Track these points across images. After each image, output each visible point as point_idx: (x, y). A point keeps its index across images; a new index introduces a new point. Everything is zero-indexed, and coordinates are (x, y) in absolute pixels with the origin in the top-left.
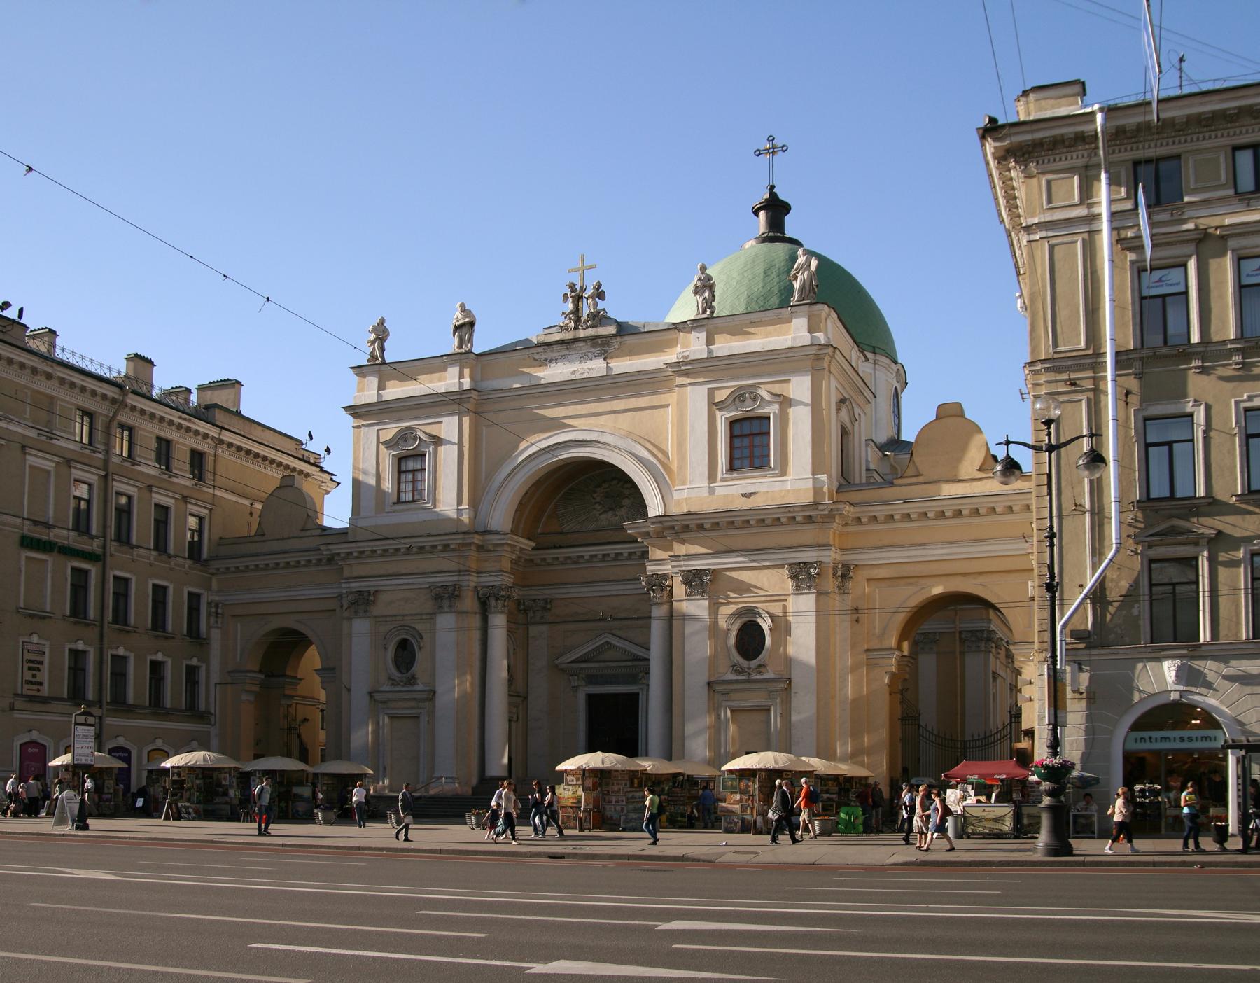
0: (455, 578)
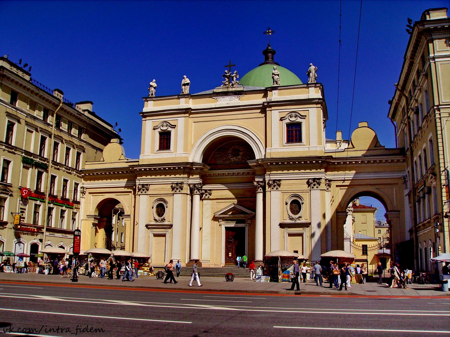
0: (182, 180)
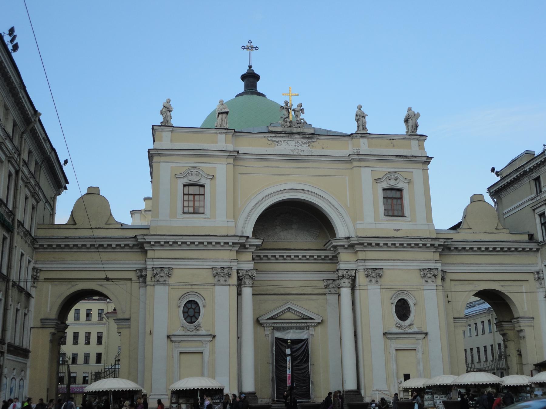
0: (228, 264)
